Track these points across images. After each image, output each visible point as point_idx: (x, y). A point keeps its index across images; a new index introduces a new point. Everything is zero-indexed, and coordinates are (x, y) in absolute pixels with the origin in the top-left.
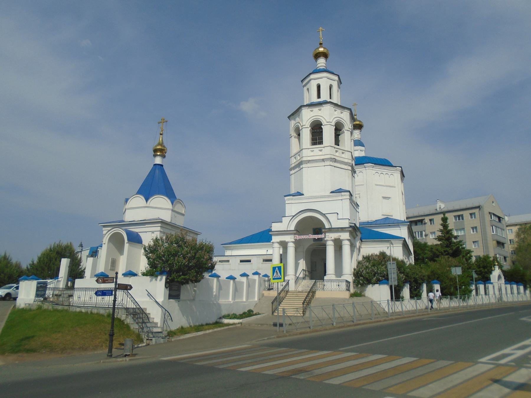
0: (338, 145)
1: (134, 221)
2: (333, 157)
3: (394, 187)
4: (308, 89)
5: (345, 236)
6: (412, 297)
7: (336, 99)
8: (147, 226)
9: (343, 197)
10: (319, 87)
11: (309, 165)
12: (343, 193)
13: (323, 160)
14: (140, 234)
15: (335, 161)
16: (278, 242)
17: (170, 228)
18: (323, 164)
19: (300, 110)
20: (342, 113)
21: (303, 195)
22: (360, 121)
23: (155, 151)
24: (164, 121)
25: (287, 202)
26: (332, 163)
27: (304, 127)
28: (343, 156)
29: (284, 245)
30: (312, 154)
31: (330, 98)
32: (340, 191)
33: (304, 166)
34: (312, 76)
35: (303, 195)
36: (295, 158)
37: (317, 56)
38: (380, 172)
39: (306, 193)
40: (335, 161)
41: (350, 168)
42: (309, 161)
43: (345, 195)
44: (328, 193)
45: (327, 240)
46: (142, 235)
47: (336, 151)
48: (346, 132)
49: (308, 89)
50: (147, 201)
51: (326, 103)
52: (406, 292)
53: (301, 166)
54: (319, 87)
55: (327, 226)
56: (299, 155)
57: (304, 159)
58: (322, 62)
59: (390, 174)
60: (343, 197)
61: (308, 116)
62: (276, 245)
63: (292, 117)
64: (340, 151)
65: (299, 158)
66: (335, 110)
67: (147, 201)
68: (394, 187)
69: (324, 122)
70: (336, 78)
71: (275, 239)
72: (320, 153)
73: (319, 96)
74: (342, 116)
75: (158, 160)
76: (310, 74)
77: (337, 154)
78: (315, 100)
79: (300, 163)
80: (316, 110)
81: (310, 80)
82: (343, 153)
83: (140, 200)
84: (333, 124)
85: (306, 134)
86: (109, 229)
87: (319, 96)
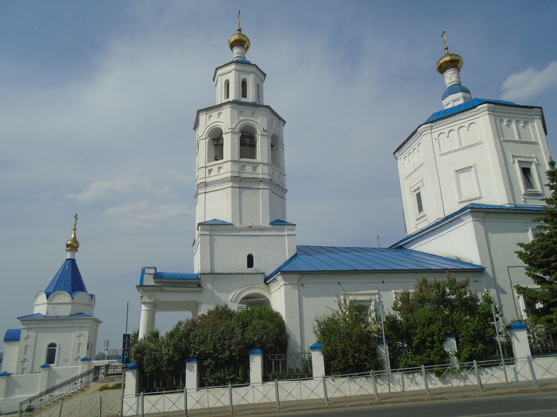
2: (203, 180)
3: (481, 143)
6: (202, 384)
20: (220, 114)
22: (450, 55)
28: (222, 171)
47: (210, 171)
52: (191, 375)
59: (466, 124)
66: (210, 116)
68: (480, 143)
82: (220, 168)
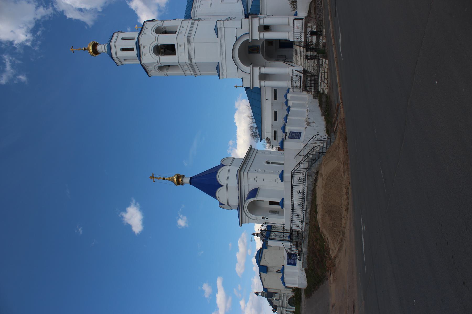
0: (176, 32)
1: (239, 197)
4: (125, 60)
5: (256, 22)
7: (135, 35)
8: (242, 184)
9: (222, 26)
10: (123, 49)
12: (218, 26)
13: (189, 44)
14: (250, 190)
15: (190, 34)
17: (245, 166)
18: (192, 45)
19: (144, 65)
20: (147, 28)
23: (178, 183)
24: (152, 177)
26: (192, 37)
27: (159, 61)
28: (185, 27)
29: (263, 77)
30: (183, 54)
31: (134, 39)
32: (216, 30)
33: (193, 61)
34: (114, 55)
36: (186, 70)
37: (95, 52)
38: (199, 4)
39: (217, 60)
40: (190, 34)
41: (197, 22)
42: (190, 57)
43: (220, 25)
44: (219, 39)
45: (260, 39)
46: (251, 189)
47: (181, 33)
48: (164, 25)
49: (125, 60)
50: (222, 186)
51: (138, 44)
53: (194, 64)
54: (123, 49)
55: (246, 38)
56: (183, 66)
57: (187, 61)
58: (101, 48)
60: (222, 26)
61: (150, 58)
62: (263, 83)
63: (149, 73)
64: (182, 29)
65: (186, 67)
67: (222, 186)
69: (155, 43)
70: (116, 34)
71: (257, 84)
72: (183, 47)
73: (132, 49)
74: (150, 28)
75: (187, 180)
76: (112, 57)
77: (184, 32)
78: (134, 53)
79: (191, 64)
80: (143, 51)
81: (117, 57)
82: (183, 27)
83: (221, 192)
84: (157, 35)
85: (166, 59)
86: (243, 213)
87: (132, 49)
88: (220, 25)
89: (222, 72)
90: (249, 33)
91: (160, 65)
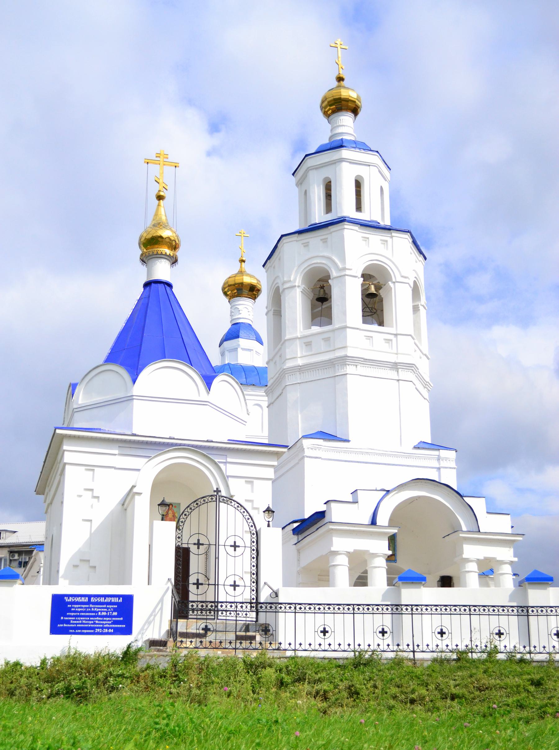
10: (358, 185)
11: (361, 370)
13: (395, 366)
16: (348, 554)
18: (392, 374)
19: (332, 228)
21: (349, 441)
25: (307, 452)
27: (348, 272)
33: (350, 369)
35: (349, 441)
54: (358, 185)
57: (350, 352)
61: (357, 251)
69: (396, 276)
72: (385, 347)
79: (344, 360)
88: (446, 459)
89: (319, 447)
90: (479, 531)
91: (334, 273)
